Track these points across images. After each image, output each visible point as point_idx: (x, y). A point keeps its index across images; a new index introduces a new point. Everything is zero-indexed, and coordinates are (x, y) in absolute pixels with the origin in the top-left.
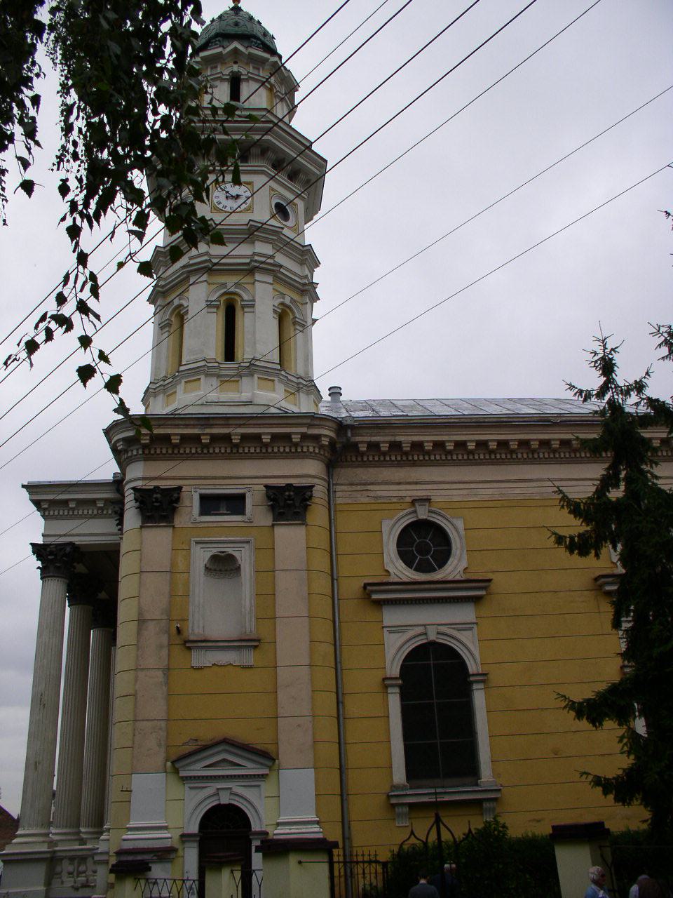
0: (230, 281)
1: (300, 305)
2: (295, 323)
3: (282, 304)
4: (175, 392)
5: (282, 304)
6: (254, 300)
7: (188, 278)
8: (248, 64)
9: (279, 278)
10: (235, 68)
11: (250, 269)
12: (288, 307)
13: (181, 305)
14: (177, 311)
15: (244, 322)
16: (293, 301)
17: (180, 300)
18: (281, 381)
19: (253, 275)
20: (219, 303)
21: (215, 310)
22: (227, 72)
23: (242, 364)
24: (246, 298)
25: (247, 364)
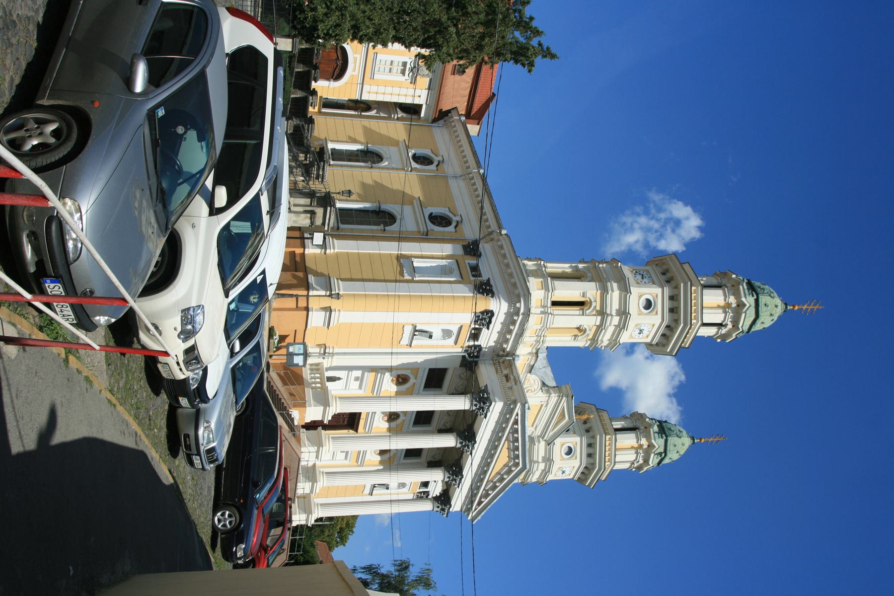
1: (586, 339)
2: (576, 336)
3: (586, 329)
6: (586, 315)
9: (599, 329)
11: (602, 313)
12: (585, 332)
13: (587, 277)
14: (585, 275)
15: (575, 310)
16: (588, 335)
17: (590, 276)
18: (542, 327)
21: (581, 295)
23: (549, 309)
24: (587, 312)
25: (549, 312)
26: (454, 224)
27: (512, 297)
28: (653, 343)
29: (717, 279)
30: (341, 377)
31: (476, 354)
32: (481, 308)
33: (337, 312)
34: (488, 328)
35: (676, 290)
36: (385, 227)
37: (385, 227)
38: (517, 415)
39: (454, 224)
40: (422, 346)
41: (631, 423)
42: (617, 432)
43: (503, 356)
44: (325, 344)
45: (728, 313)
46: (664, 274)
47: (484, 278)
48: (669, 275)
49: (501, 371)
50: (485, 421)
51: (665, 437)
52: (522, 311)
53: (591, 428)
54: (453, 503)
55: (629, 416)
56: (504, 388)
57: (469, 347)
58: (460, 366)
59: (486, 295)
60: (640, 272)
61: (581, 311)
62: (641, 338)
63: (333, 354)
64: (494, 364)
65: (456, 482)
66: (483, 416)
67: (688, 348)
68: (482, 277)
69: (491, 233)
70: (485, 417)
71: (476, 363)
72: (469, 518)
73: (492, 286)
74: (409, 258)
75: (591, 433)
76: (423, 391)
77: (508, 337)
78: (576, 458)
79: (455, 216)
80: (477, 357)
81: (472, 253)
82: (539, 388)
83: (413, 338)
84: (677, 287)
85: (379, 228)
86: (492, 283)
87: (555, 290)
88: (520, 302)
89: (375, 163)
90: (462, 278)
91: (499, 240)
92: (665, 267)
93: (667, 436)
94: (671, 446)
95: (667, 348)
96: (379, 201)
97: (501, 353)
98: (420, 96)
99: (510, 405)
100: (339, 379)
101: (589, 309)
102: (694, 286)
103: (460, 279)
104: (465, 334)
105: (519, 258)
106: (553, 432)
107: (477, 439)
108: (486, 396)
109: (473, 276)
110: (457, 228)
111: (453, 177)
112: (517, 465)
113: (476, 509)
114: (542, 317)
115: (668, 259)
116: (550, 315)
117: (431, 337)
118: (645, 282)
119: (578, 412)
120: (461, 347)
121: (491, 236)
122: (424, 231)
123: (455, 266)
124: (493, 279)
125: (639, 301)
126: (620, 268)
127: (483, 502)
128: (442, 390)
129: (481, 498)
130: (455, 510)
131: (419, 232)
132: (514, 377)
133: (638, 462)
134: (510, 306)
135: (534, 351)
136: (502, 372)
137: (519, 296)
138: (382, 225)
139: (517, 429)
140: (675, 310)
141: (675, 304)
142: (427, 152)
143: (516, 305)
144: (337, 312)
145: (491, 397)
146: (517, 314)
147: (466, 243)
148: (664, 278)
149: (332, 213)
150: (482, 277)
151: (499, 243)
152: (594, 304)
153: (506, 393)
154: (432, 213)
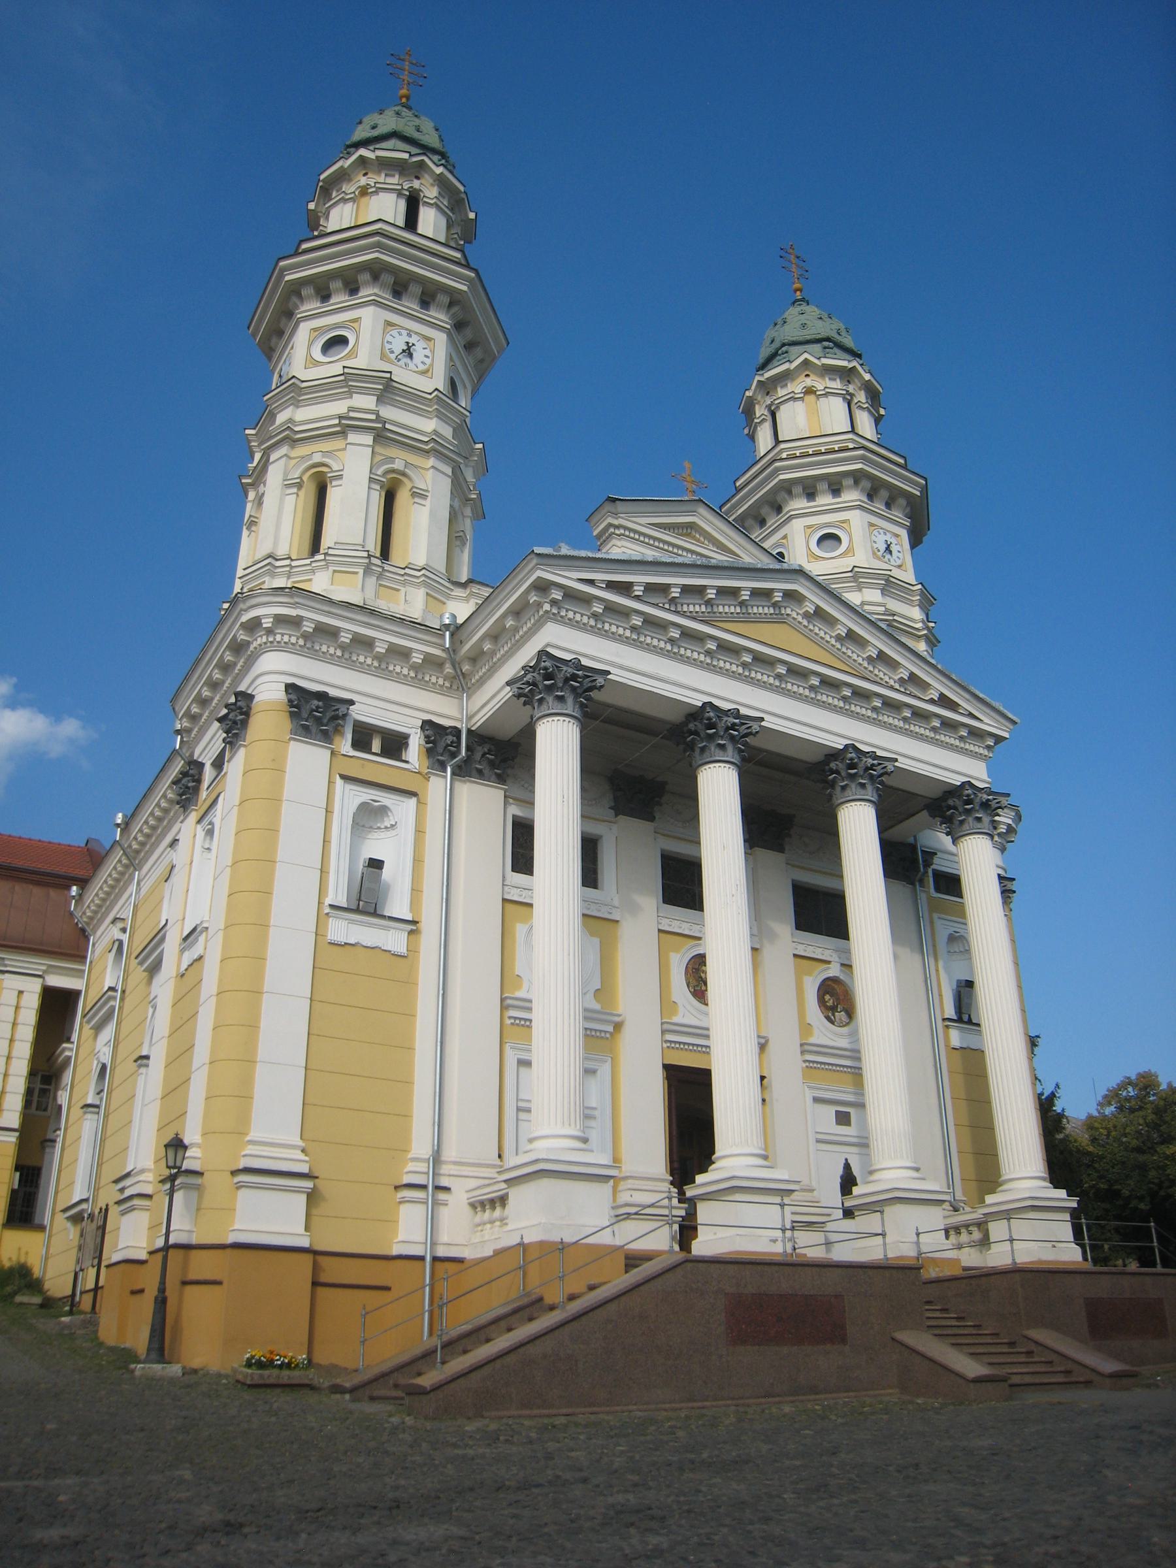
0: (315, 452)
5: (393, 471)
8: (379, 172)
12: (404, 474)
16: (407, 464)
19: (346, 438)
20: (298, 481)
21: (295, 490)
24: (335, 467)
28: (449, 327)
31: (450, 739)
33: (250, 1149)
35: (304, 292)
38: (591, 582)
40: (416, 891)
44: (396, 1188)
45: (377, 185)
50: (617, 675)
51: (784, 349)
57: (426, 763)
61: (334, 483)
62: (433, 352)
63: (437, 1158)
65: (873, 765)
72: (1006, 735)
74: (182, 951)
76: (603, 890)
78: (844, 522)
80: (457, 732)
83: (383, 917)
93: (784, 345)
94: (805, 332)
98: (21, 992)
99: (554, 602)
104: (374, 764)
113: (971, 716)
114: (335, 571)
116: (331, 552)
117: (376, 864)
120: (428, 779)
127: (942, 696)
130: (985, 777)
133: (852, 395)
135: (458, 592)
139: (650, 588)
143: (269, 631)
144: (250, 1149)
146: (296, 622)
152: (317, 458)
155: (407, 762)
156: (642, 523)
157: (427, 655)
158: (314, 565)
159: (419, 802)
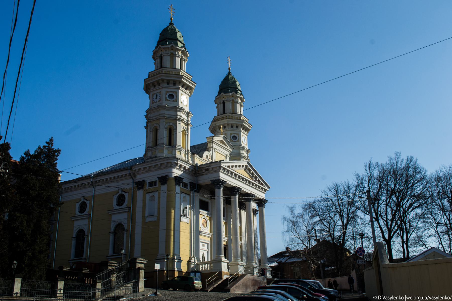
3: (183, 129)
4: (156, 151)
6: (177, 128)
7: (159, 119)
10: (172, 52)
13: (156, 126)
14: (155, 128)
21: (166, 130)
22: (170, 53)
24: (175, 128)
26: (123, 193)
27: (168, 166)
28: (189, 94)
29: (157, 58)
30: (203, 253)
32: (174, 183)
34: (183, 179)
36: (125, 229)
37: (125, 229)
38: (226, 166)
39: (123, 193)
41: (221, 105)
42: (226, 113)
43: (195, 172)
46: (155, 86)
47: (157, 180)
48: (156, 83)
49: (203, 173)
50: (228, 182)
52: (176, 162)
53: (223, 126)
54: (262, 198)
55: (216, 105)
56: (212, 172)
58: (199, 193)
59: (167, 179)
60: (153, 99)
61: (175, 131)
64: (199, 176)
66: (226, 183)
67: (192, 77)
68: (156, 181)
69: (130, 174)
70: (226, 182)
71: (198, 185)
73: (162, 176)
74: (144, 217)
75: (226, 125)
77: (187, 169)
79: (119, 192)
80: (195, 184)
81: (143, 185)
82: (209, 153)
84: (163, 80)
85: (125, 233)
86: (161, 176)
87: (164, 143)
88: (171, 162)
89: (85, 234)
90: (157, 191)
91: (135, 170)
92: (151, 85)
93: (228, 87)
95: (192, 87)
96: (109, 233)
97: (194, 172)
100: (203, 254)
101: (173, 126)
102: (162, 71)
103: (157, 192)
105: (146, 161)
106: (228, 146)
107: (235, 186)
108: (216, 182)
109: (155, 185)
110: (126, 191)
111: (94, 192)
112: (246, 166)
115: (147, 83)
118: (160, 96)
119: (214, 131)
120: (190, 192)
121: (132, 174)
122: (128, 209)
123: (150, 194)
124: (158, 175)
125: (170, 101)
126: (152, 109)
128: (209, 202)
129: (260, 184)
131: (128, 211)
132: (207, 167)
134: (174, 167)
136: (204, 172)
137: (167, 163)
138: (124, 231)
140: (174, 83)
141: (172, 82)
142: (78, 205)
143: (173, 164)
145: (217, 179)
147: (136, 188)
148: (157, 86)
149: (139, 259)
150: (156, 181)
151: (137, 170)
152: (171, 124)
153: (216, 171)
154: (117, 204)
155: (188, 189)
156: (216, 140)
157: (192, 170)
158: (173, 148)
159: (190, 197)
